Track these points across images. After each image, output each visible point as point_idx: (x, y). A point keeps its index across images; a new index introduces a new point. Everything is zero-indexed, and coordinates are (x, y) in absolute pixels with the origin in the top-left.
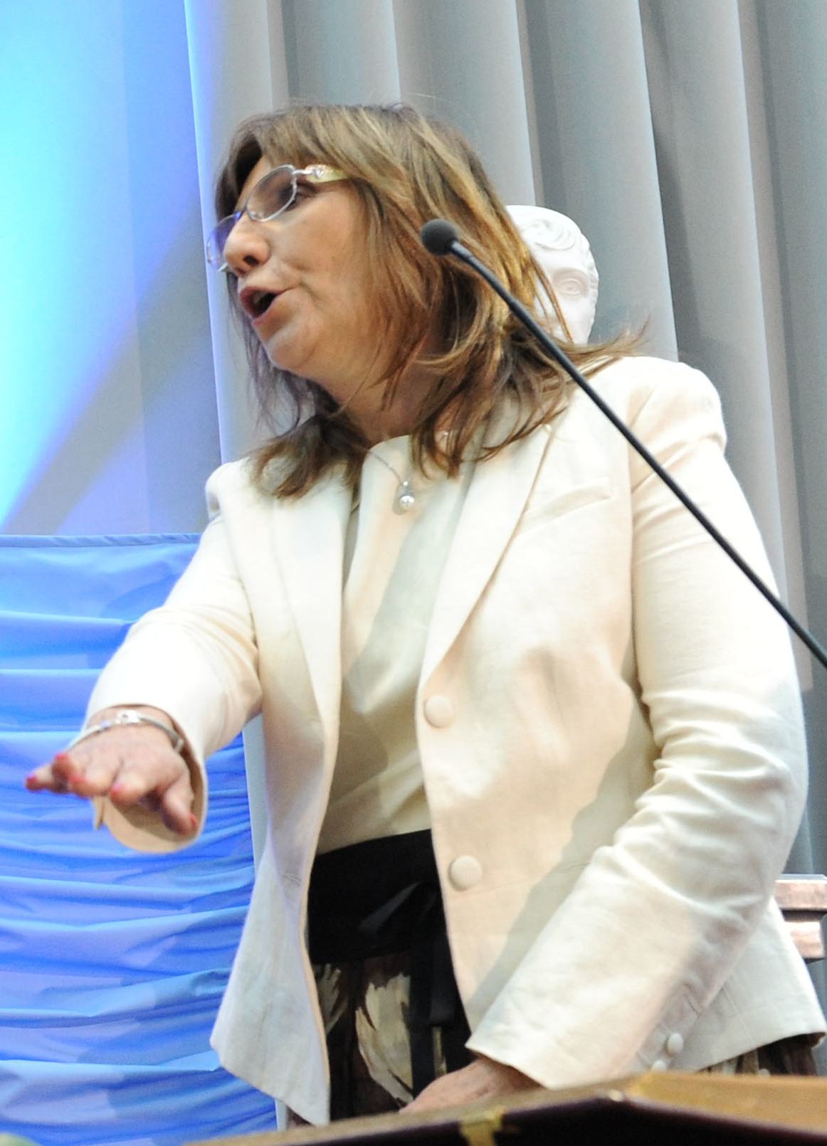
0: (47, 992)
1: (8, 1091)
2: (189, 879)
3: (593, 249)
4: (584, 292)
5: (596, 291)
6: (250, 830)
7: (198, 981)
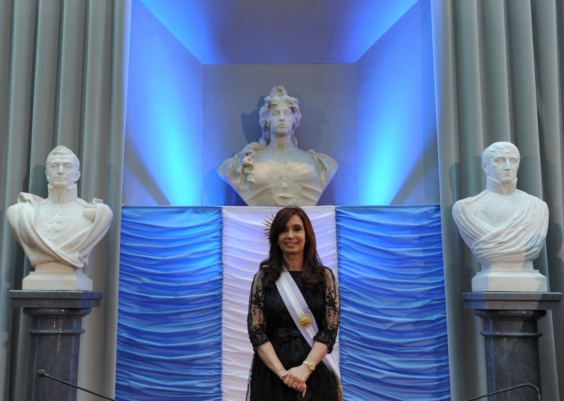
0: (401, 302)
1: (391, 324)
2: (430, 279)
6: (443, 269)
7: (432, 301)
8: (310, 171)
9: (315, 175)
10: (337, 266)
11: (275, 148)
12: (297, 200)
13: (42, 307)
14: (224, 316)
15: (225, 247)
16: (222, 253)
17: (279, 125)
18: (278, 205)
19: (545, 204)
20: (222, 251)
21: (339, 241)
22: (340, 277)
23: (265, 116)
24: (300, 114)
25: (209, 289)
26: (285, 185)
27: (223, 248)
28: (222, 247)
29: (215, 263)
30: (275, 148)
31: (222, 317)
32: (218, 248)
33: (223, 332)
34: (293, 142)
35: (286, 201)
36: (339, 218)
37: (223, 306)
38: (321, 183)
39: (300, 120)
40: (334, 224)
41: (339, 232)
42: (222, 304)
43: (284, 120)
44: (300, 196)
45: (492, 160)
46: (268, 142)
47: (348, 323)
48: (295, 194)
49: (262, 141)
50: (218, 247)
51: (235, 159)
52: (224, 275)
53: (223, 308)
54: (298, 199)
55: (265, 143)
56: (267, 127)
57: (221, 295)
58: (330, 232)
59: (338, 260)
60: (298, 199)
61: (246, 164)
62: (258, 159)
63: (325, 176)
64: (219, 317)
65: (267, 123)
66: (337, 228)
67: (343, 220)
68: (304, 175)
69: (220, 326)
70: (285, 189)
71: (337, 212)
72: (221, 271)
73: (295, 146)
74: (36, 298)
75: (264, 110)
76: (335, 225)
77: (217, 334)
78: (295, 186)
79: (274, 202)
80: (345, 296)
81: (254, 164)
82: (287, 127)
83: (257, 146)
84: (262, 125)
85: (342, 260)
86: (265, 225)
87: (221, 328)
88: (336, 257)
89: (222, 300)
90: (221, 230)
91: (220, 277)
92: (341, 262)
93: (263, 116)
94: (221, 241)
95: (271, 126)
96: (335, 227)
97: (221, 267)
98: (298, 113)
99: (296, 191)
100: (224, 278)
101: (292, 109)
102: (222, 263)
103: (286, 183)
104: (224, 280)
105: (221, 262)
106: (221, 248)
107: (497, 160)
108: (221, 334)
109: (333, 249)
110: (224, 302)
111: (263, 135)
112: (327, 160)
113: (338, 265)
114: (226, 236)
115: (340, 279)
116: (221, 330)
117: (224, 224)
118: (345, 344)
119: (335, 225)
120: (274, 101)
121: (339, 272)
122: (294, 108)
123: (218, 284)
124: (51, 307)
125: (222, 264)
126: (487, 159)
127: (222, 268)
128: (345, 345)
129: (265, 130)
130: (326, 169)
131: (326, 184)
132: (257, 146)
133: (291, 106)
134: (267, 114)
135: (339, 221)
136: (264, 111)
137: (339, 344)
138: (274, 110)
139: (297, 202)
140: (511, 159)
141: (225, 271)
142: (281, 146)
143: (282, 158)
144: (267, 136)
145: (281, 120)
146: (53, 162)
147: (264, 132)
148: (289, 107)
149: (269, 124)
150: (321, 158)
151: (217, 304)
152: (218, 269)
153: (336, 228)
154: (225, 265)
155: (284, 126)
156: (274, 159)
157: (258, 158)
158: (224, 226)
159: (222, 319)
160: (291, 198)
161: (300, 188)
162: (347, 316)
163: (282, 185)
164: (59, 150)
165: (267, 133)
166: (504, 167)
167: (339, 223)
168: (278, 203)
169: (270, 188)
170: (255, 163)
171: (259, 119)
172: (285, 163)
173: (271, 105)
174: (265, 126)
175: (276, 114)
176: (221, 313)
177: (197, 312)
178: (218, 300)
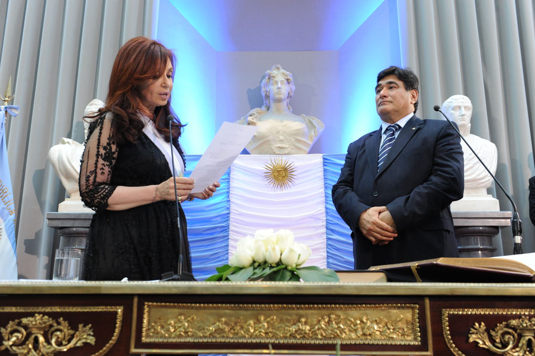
3: (472, 102)
4: (470, 110)
5: (472, 110)
8: (302, 127)
9: (306, 130)
10: (325, 202)
11: (274, 111)
12: (291, 149)
13: (74, 226)
14: (230, 244)
15: (232, 188)
16: (229, 193)
17: (277, 92)
18: (276, 153)
19: (493, 145)
20: (229, 191)
21: (326, 182)
22: (327, 211)
23: (266, 87)
24: (294, 86)
25: (218, 222)
26: (281, 138)
27: (230, 188)
28: (229, 187)
29: (224, 200)
30: (274, 111)
31: (229, 244)
32: (226, 188)
33: (229, 257)
34: (289, 109)
35: (282, 150)
36: (326, 164)
37: (229, 235)
38: (311, 138)
39: (294, 91)
40: (322, 169)
41: (326, 175)
42: (229, 234)
43: (281, 88)
44: (294, 147)
45: (450, 109)
46: (268, 109)
47: (334, 249)
48: (290, 145)
49: (264, 108)
50: (227, 187)
51: (242, 120)
52: (231, 210)
53: (230, 237)
54: (292, 149)
55: (266, 109)
56: (267, 95)
57: (228, 226)
58: (318, 174)
59: (326, 197)
60: (292, 149)
61: (250, 122)
62: (260, 120)
63: (314, 132)
64: (226, 244)
65: (267, 92)
66: (324, 172)
67: (328, 165)
68: (297, 130)
69: (227, 252)
70: (281, 141)
71: (324, 159)
72: (228, 206)
73: (290, 112)
74: (69, 218)
75: (265, 82)
76: (323, 169)
77: (225, 259)
78: (289, 138)
79: (273, 151)
80: (332, 226)
81: (257, 123)
82: (283, 94)
83: (259, 111)
84: (263, 94)
85: (329, 198)
86: (265, 169)
87: (227, 253)
88: (323, 195)
89: (229, 231)
90: (229, 174)
91: (228, 212)
92: (328, 199)
93: (264, 87)
94: (229, 182)
95: (270, 94)
96: (322, 171)
97: (229, 203)
98: (292, 84)
99: (290, 142)
100: (230, 213)
101: (287, 80)
102: (230, 200)
103: (282, 136)
104: (231, 214)
105: (228, 199)
106: (229, 188)
107: (454, 109)
108: (228, 259)
109: (322, 188)
110: (230, 233)
111: (264, 104)
112: (315, 121)
113: (325, 201)
114: (233, 178)
115: (328, 213)
116: (228, 255)
117: (231, 169)
118: (332, 266)
119: (323, 169)
120: (273, 74)
121: (326, 207)
122: (289, 79)
123: (227, 217)
124: (81, 226)
125: (229, 201)
126: (447, 109)
127: (230, 205)
128: (332, 267)
129: (266, 99)
130: (315, 127)
131: (315, 139)
132: (259, 111)
133: (286, 78)
134: (267, 85)
135: (326, 166)
136: (265, 82)
137: (327, 266)
138: (273, 80)
139: (292, 151)
140: (465, 107)
141: (232, 207)
142: (278, 110)
143: (279, 118)
144: (267, 103)
145: (279, 88)
146: (89, 110)
147: (265, 100)
148: (285, 79)
149: (269, 93)
150: (311, 120)
151: (225, 234)
152: (226, 205)
153: (323, 171)
154: (232, 202)
155: (281, 93)
156: (273, 119)
157: (259, 119)
158: (232, 170)
159: (229, 246)
160: (286, 148)
161: (294, 140)
162: (334, 244)
163: (279, 138)
164: (95, 102)
165: (267, 101)
166: (460, 113)
167: (326, 168)
168: (275, 151)
169: (269, 140)
170: (257, 122)
171: (261, 90)
172: (282, 122)
173: (270, 77)
174: (266, 95)
175: (274, 84)
176: (229, 242)
177: (208, 241)
178: (226, 231)
